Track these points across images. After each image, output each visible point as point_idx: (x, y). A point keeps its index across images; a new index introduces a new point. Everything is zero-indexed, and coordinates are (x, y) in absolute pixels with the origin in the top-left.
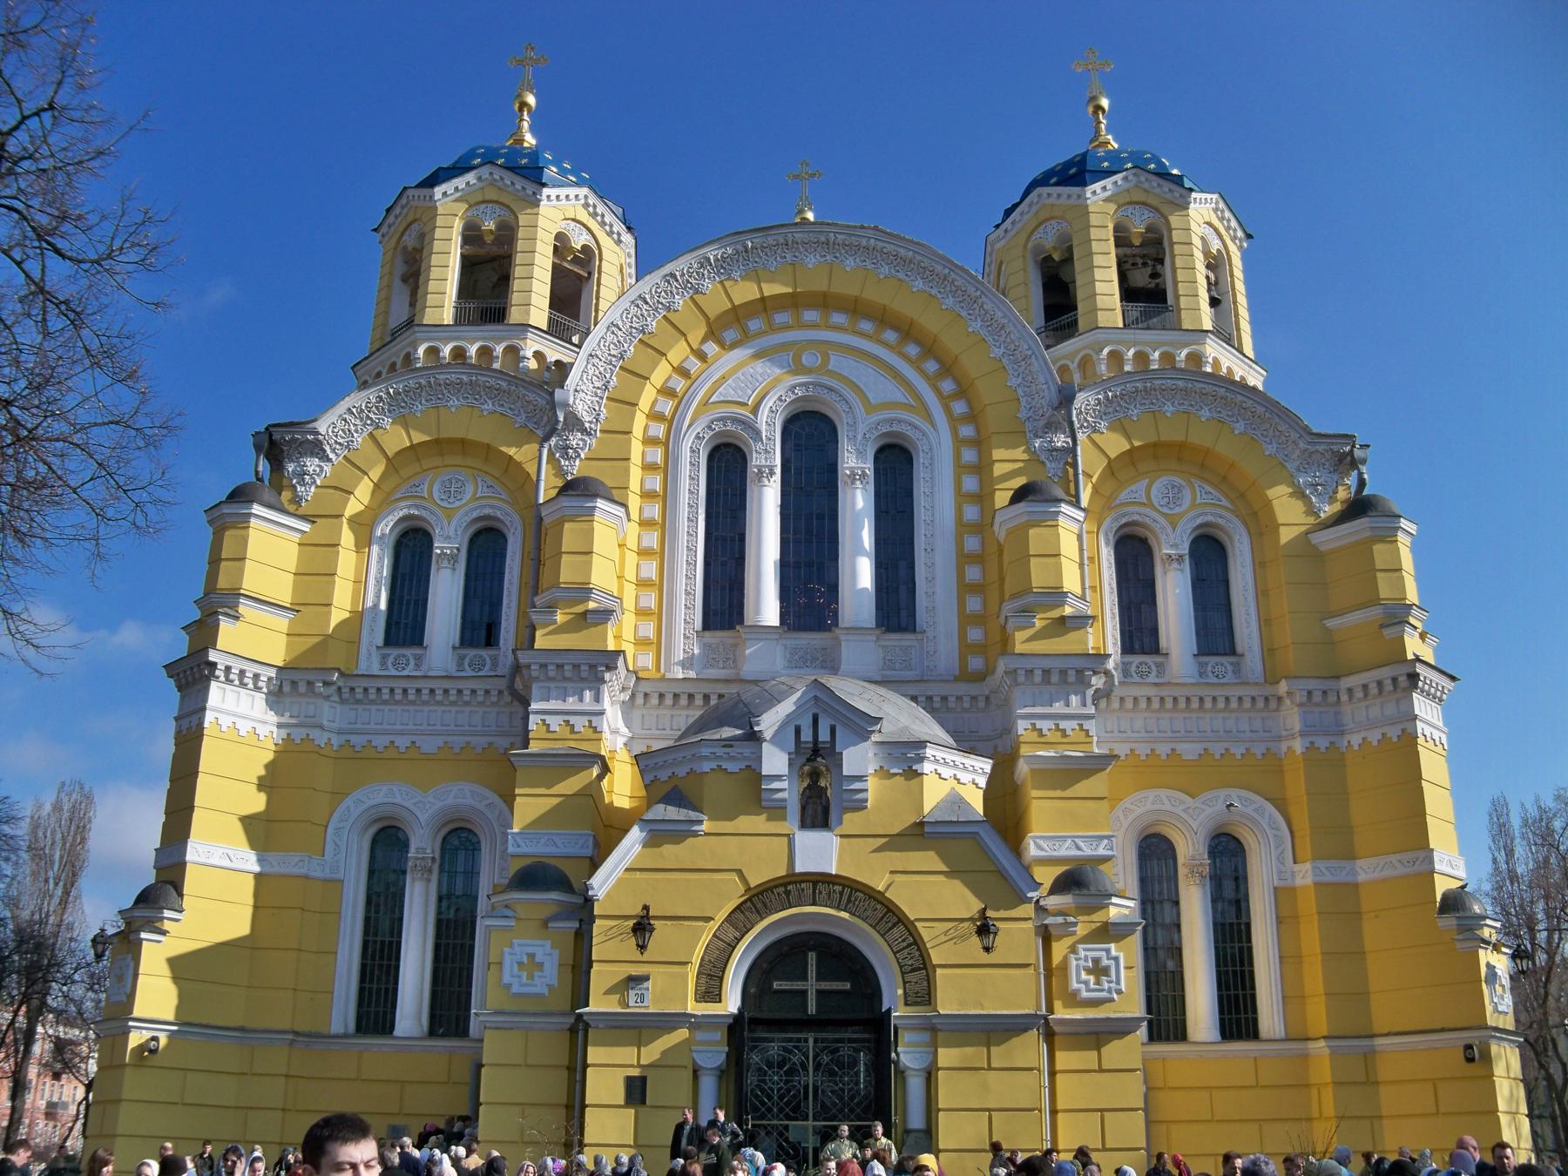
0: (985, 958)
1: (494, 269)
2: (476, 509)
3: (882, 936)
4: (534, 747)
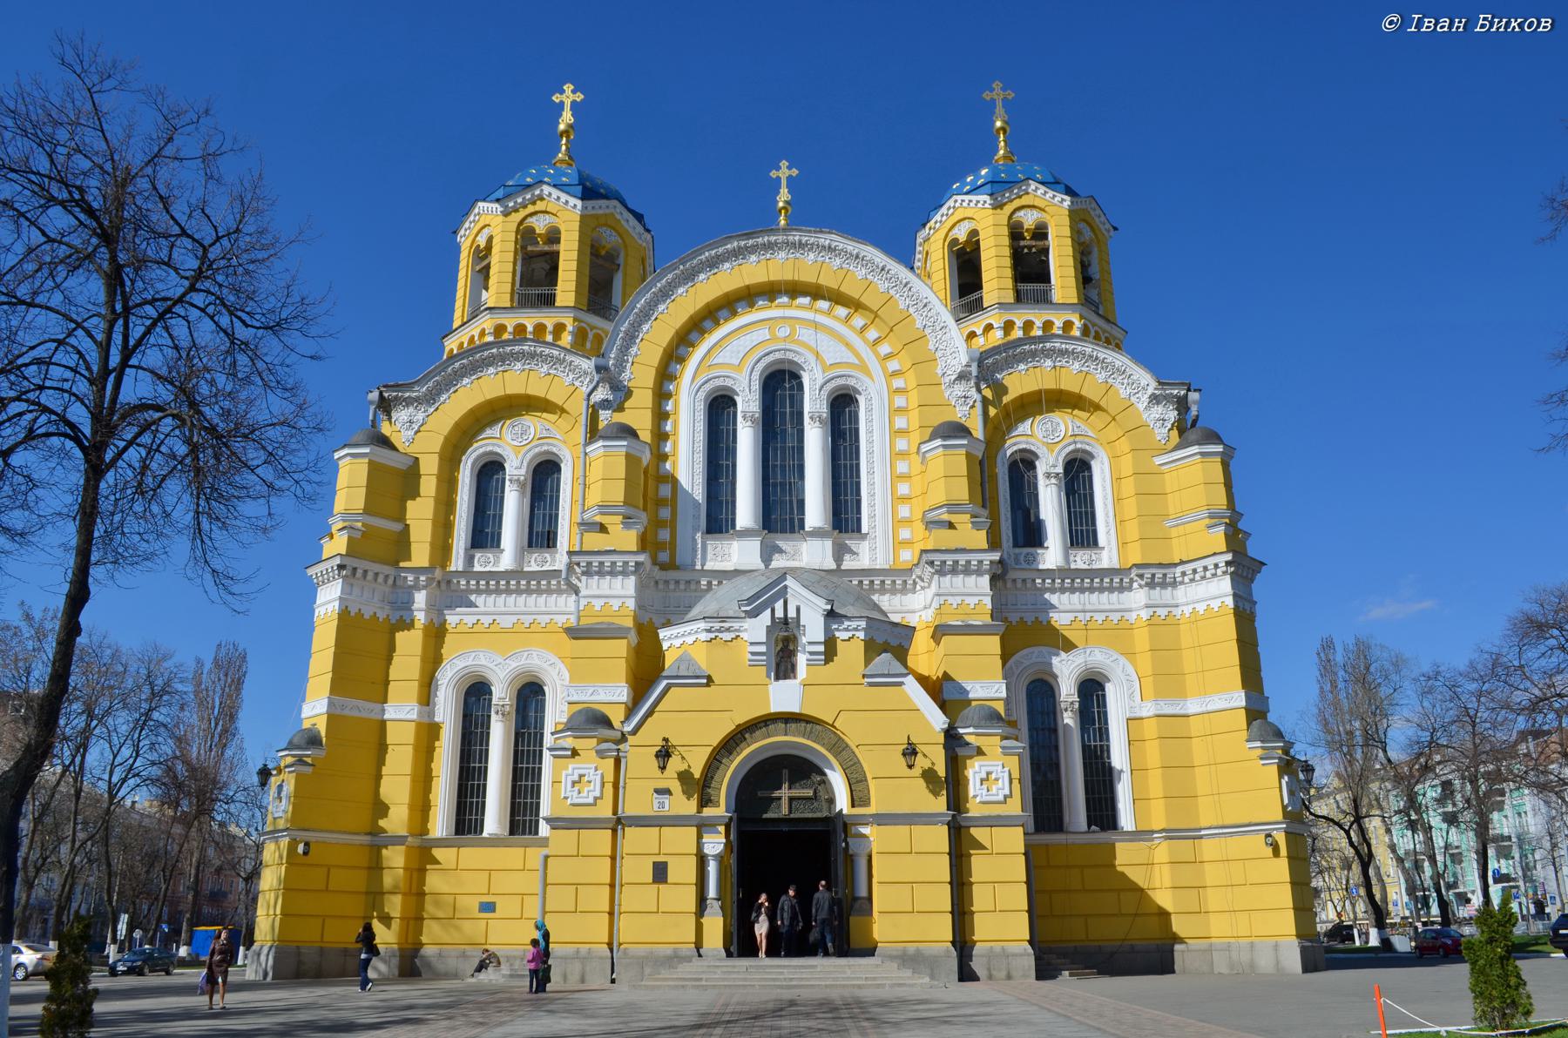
1: (546, 261)
2: (536, 446)
3: (835, 757)
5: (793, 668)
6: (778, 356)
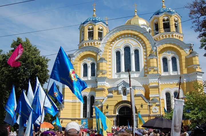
0: (142, 109)
4: (98, 88)
5: (126, 94)
6: (126, 45)
